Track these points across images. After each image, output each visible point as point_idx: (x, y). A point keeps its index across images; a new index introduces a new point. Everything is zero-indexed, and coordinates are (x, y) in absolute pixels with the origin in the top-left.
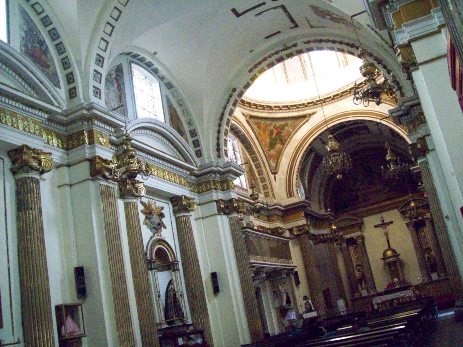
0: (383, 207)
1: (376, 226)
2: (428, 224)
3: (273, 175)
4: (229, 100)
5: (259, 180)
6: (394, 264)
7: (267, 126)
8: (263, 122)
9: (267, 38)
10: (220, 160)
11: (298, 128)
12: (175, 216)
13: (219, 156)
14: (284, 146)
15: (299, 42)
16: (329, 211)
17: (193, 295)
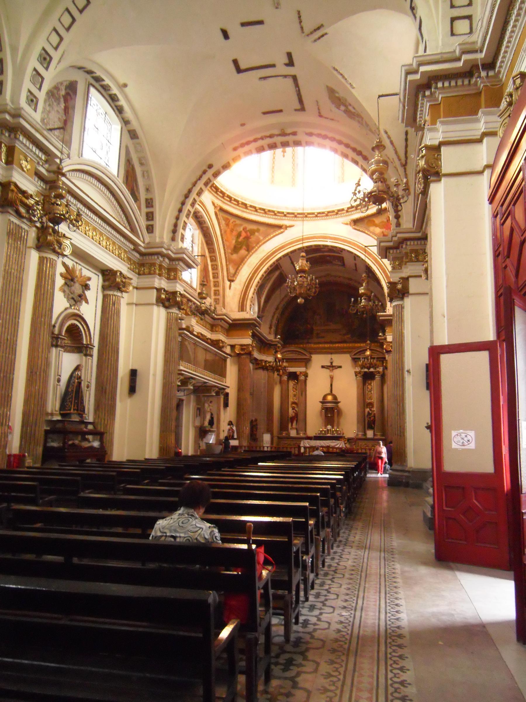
0: (334, 348)
1: (323, 367)
2: (378, 378)
4: (201, 177)
5: (212, 284)
6: (331, 411)
7: (235, 225)
8: (232, 220)
9: (264, 113)
10: (173, 244)
11: (269, 237)
12: (103, 292)
13: (173, 239)
14: (249, 253)
15: (300, 130)
16: (279, 338)
17: (102, 388)
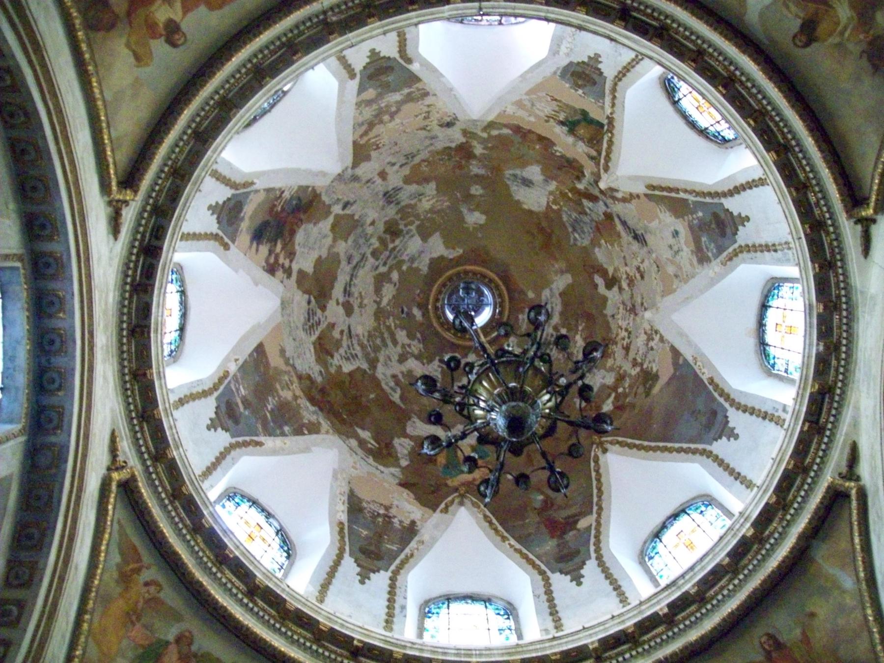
7: (154, 603)
8: (152, 572)
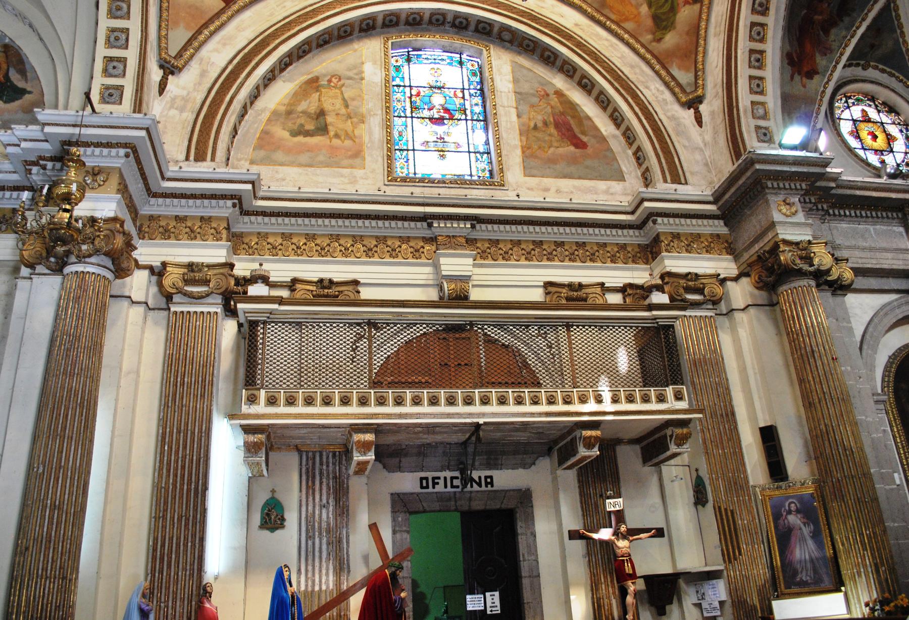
3: (692, 110)
